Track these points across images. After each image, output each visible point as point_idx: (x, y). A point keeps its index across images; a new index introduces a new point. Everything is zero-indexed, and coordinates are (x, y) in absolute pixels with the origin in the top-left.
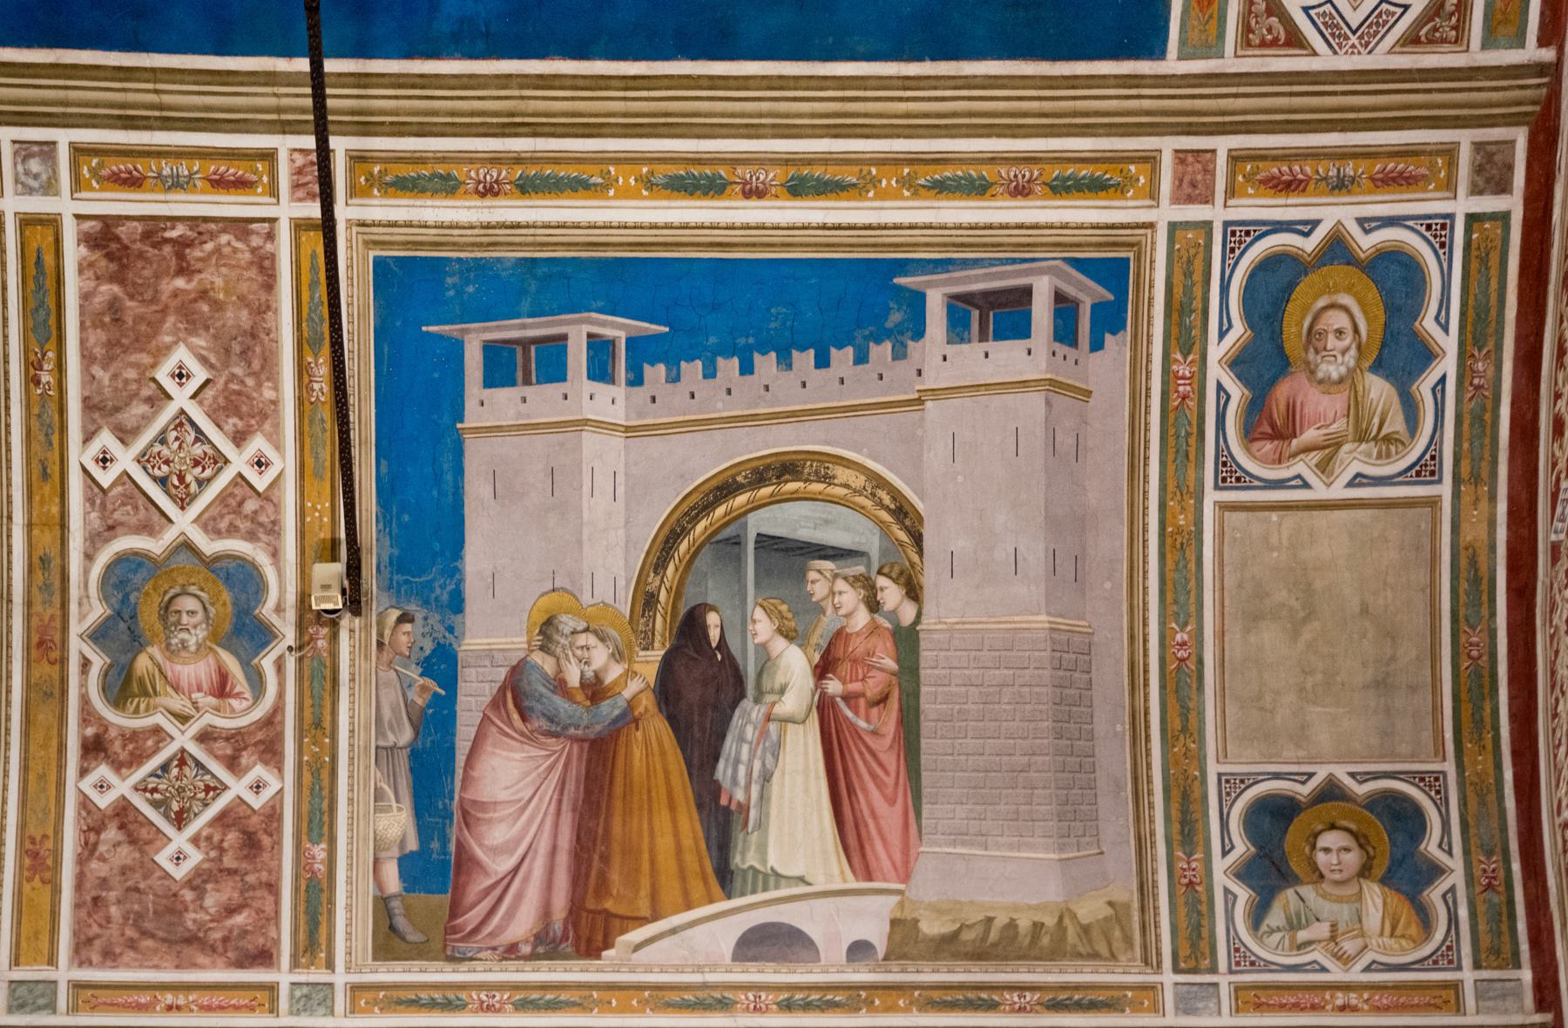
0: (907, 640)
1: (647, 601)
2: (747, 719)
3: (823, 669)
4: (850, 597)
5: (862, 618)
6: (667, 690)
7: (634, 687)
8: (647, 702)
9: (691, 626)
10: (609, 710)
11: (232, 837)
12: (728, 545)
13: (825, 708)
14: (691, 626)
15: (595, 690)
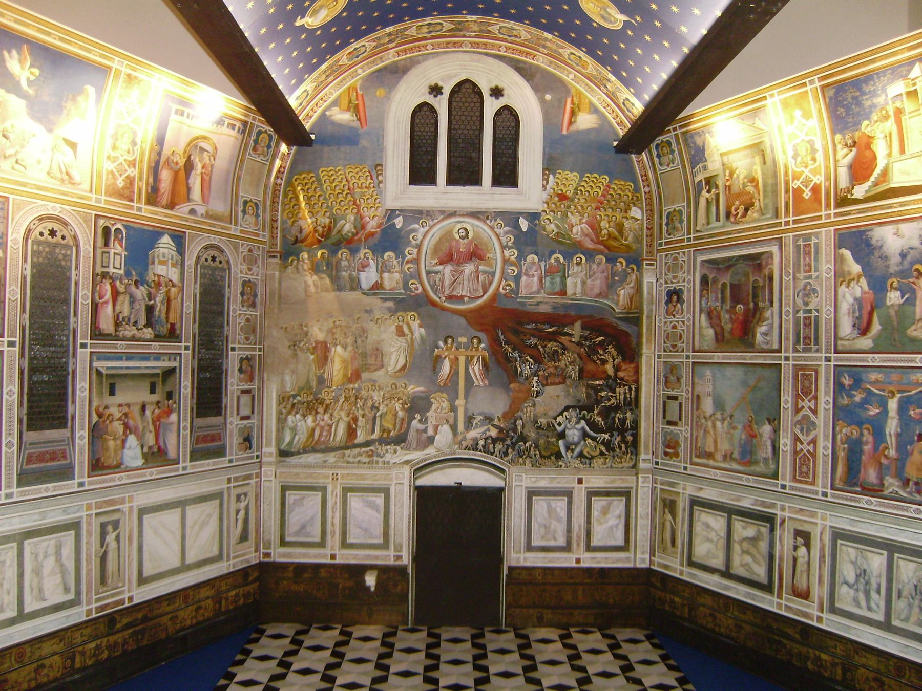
0: (212, 166)
1: (185, 152)
2: (193, 173)
3: (203, 168)
4: (207, 158)
5: (208, 162)
6: (185, 166)
7: (181, 164)
8: (183, 168)
9: (189, 157)
10: (178, 167)
11: (128, 181)
12: (196, 146)
13: (202, 174)
14: (189, 157)
15: (177, 163)
